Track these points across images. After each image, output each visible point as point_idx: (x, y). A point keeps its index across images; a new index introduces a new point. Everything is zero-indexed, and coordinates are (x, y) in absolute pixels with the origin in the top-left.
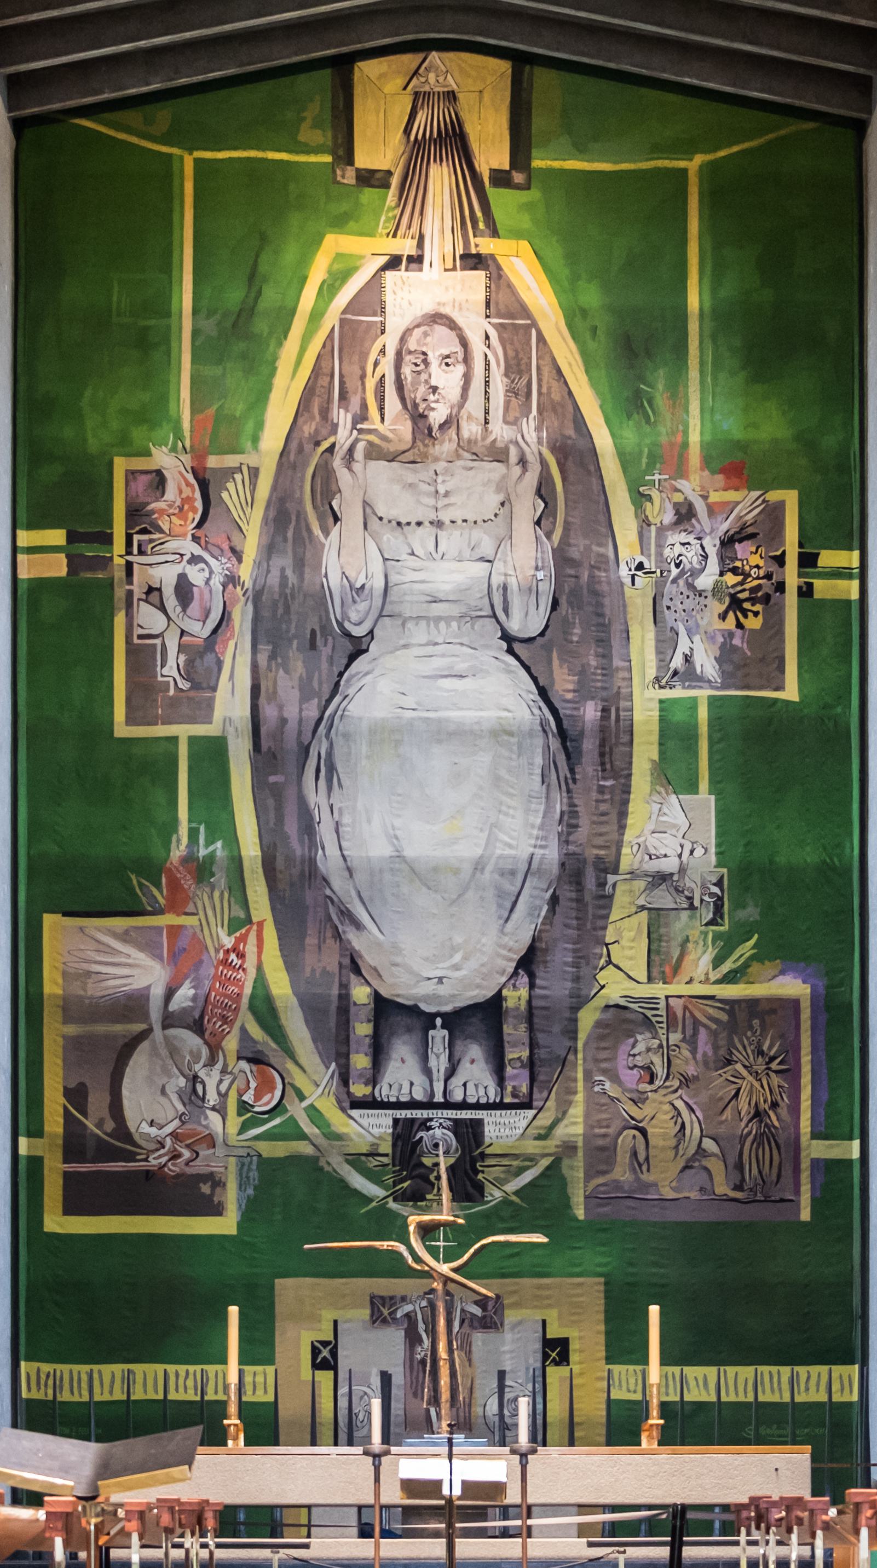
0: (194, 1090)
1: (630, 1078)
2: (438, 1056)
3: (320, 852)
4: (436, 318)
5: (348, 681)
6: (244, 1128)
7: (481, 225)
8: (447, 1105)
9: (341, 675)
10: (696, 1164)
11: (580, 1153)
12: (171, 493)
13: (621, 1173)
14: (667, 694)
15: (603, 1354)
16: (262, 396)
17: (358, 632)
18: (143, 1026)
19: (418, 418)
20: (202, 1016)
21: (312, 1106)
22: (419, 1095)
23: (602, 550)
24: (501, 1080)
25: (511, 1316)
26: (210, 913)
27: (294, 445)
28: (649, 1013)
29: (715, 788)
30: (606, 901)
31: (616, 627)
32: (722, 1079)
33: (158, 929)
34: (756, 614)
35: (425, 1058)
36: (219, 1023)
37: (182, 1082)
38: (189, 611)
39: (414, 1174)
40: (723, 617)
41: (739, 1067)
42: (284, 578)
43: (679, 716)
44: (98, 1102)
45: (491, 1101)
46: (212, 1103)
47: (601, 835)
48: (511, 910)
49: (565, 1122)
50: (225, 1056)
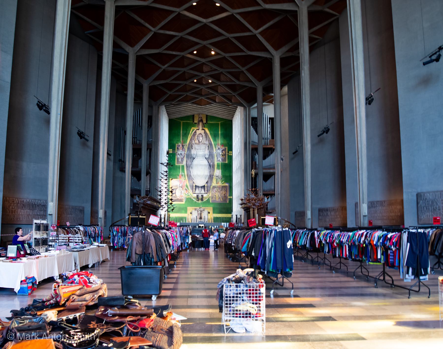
1: (215, 192)
4: (200, 134)
13: (214, 199)
17: (194, 157)
19: (199, 141)
29: (221, 169)
30: (213, 178)
43: (218, 164)
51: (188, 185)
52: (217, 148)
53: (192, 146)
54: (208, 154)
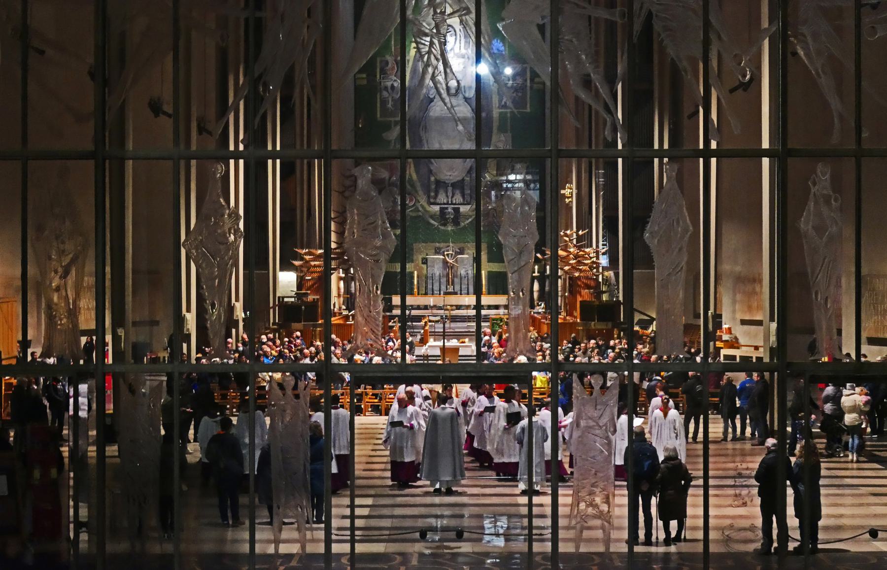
8: (452, 204)
12: (390, 65)
22: (445, 202)
35: (447, 193)
37: (393, 199)
40: (513, 93)
51: (414, 176)
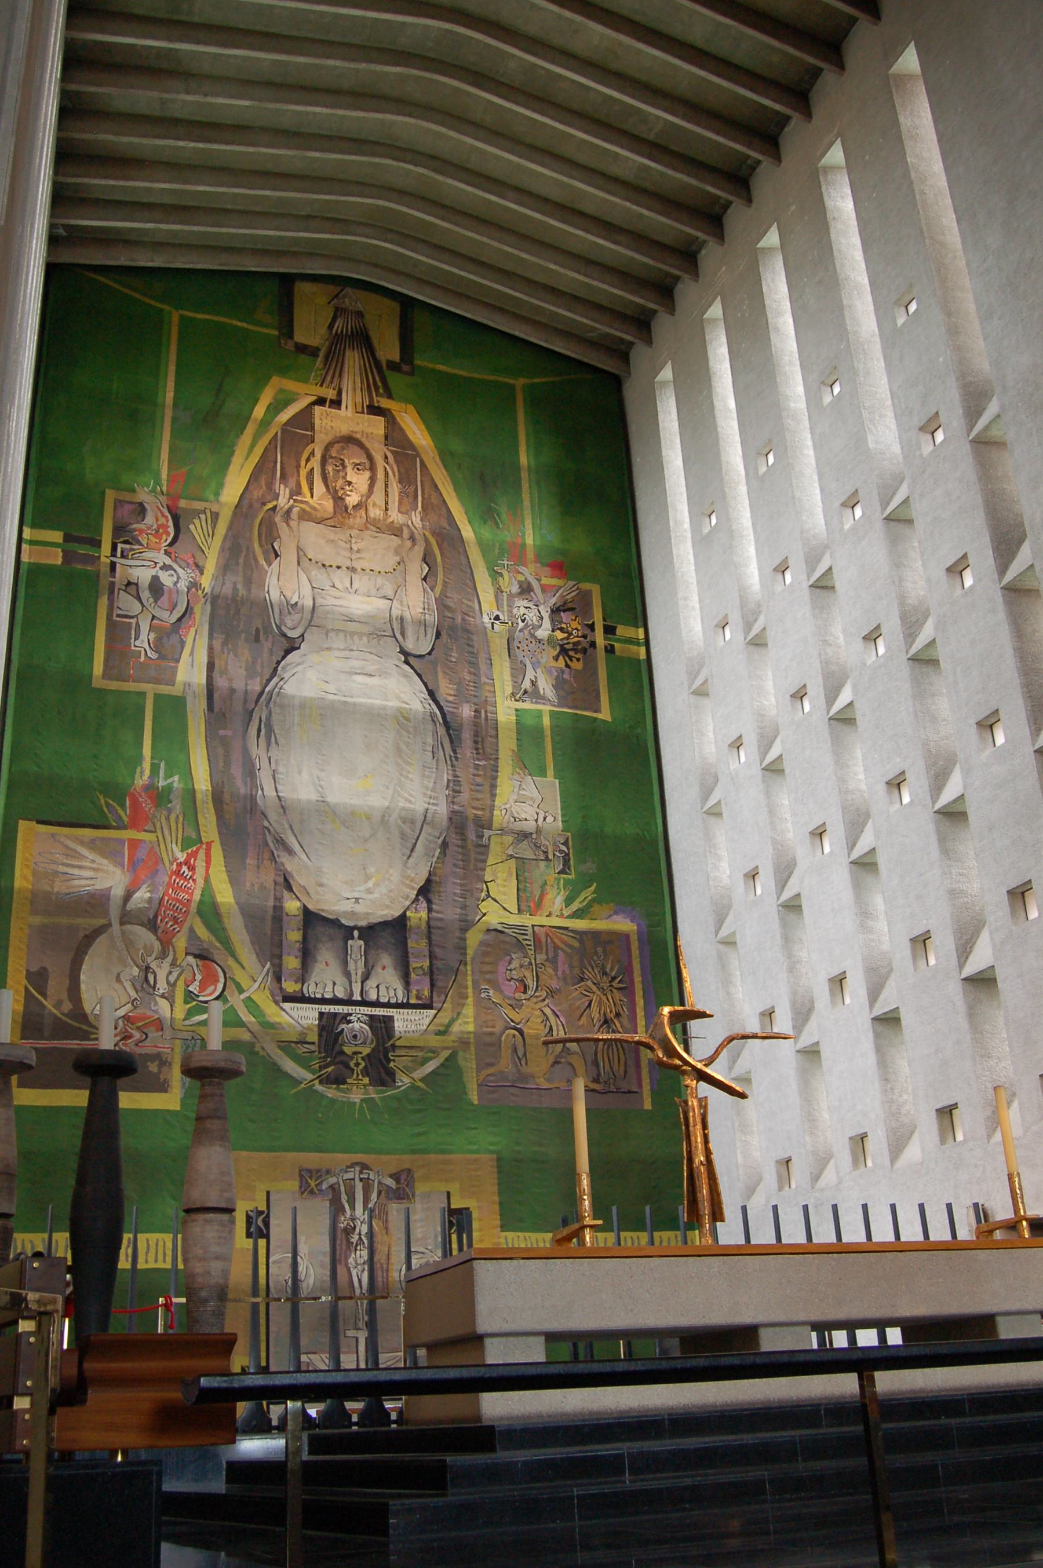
0: (146, 980)
2: (356, 962)
3: (260, 792)
4: (349, 440)
5: (283, 668)
6: (189, 1014)
7: (381, 391)
9: (279, 663)
10: (563, 1060)
11: (473, 1049)
12: (149, 519)
14: (520, 705)
15: (499, 1222)
16: (223, 467)
17: (292, 634)
18: (103, 921)
19: (338, 499)
20: (156, 916)
21: (249, 998)
22: (340, 994)
23: (470, 603)
24: (407, 983)
25: (420, 1188)
26: (166, 832)
27: (245, 502)
28: (520, 937)
31: (482, 657)
32: (577, 993)
33: (121, 842)
34: (578, 660)
35: (345, 963)
36: (171, 923)
37: (136, 971)
38: (159, 603)
39: (337, 1060)
40: (556, 658)
41: (589, 983)
42: (235, 589)
43: (530, 721)
44: (57, 986)
45: (400, 1001)
46: (161, 991)
47: (478, 800)
48: (412, 850)
49: (459, 1021)
50: (174, 951)
52: (510, 584)
53: (269, 534)
54: (432, 618)
